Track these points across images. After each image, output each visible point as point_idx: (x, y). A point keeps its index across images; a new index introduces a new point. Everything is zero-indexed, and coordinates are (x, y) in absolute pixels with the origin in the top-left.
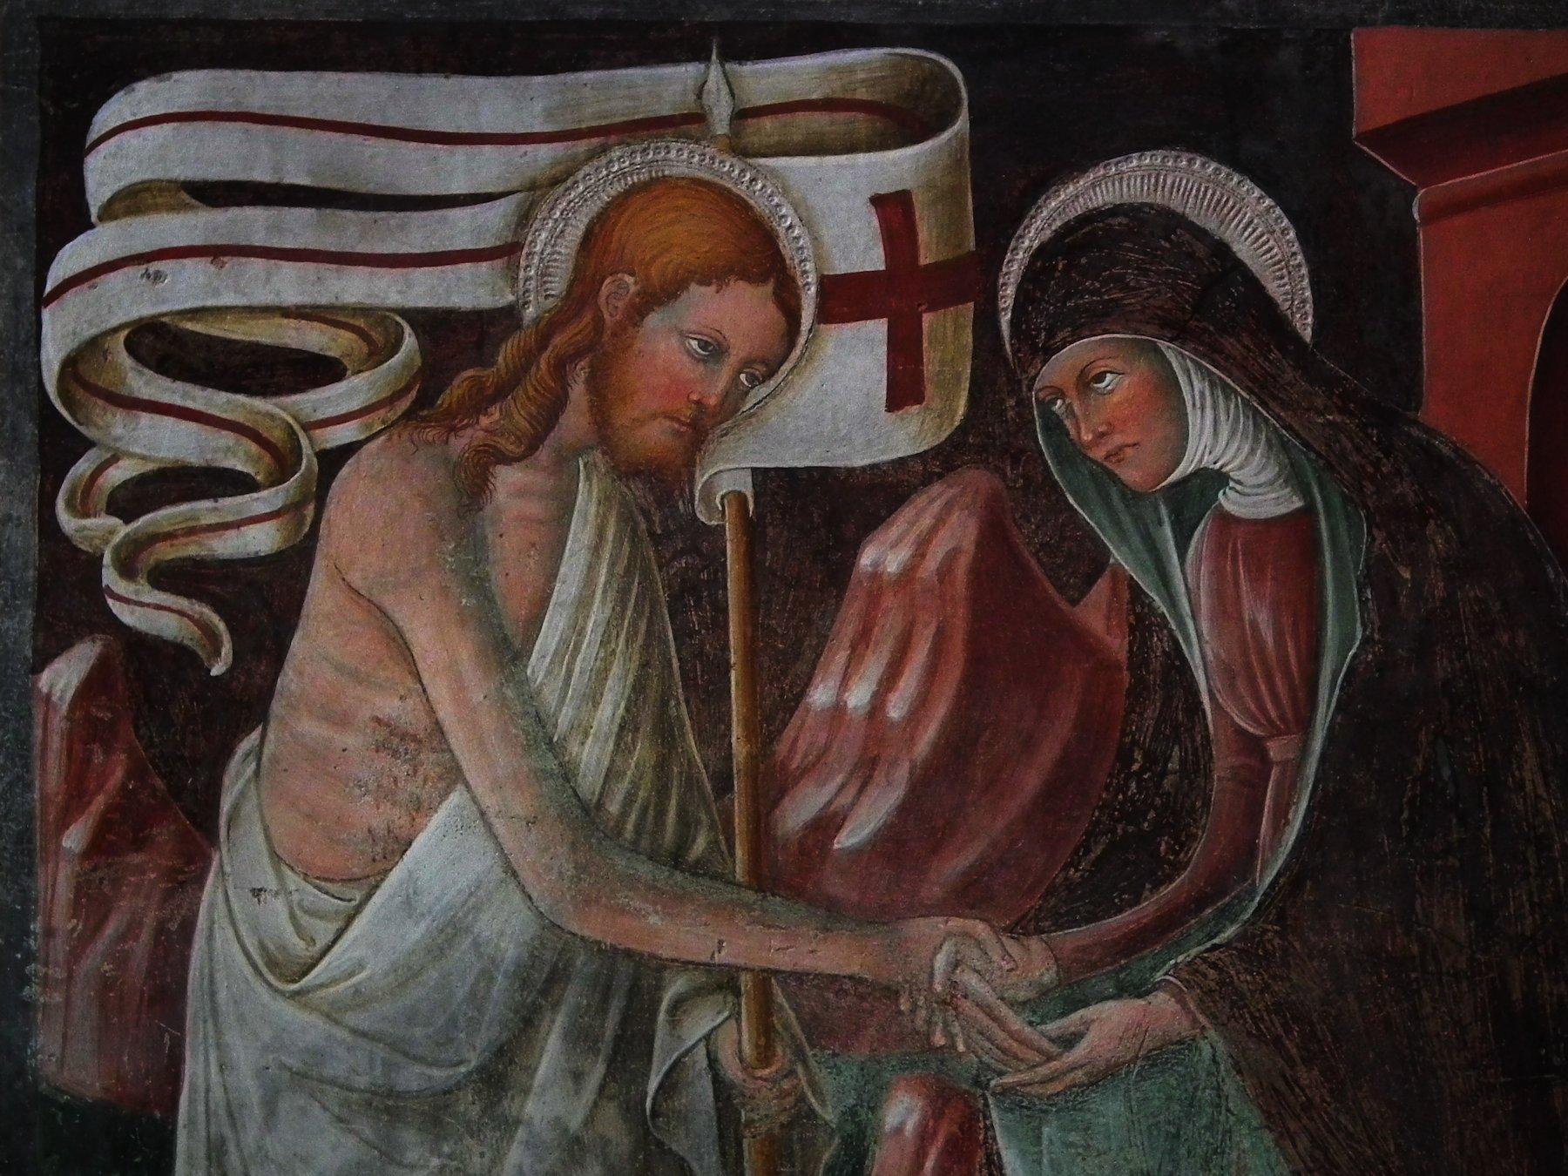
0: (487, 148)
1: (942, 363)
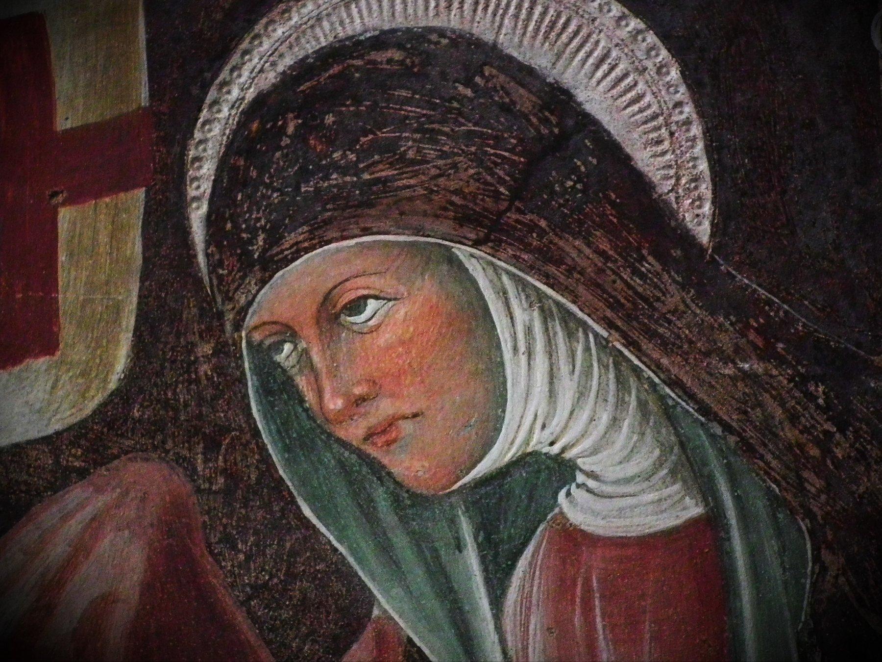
1: (91, 286)
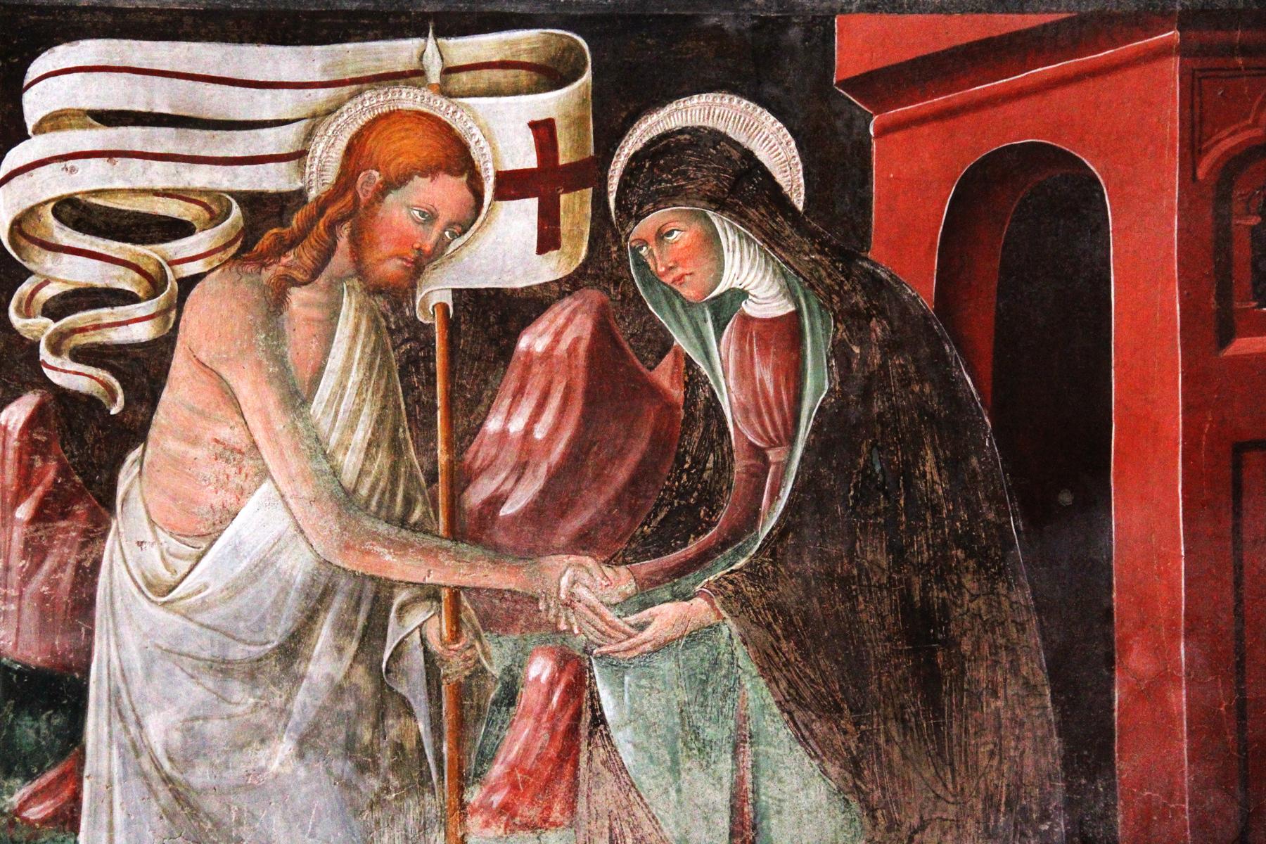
0: (285, 91)
1: (572, 224)
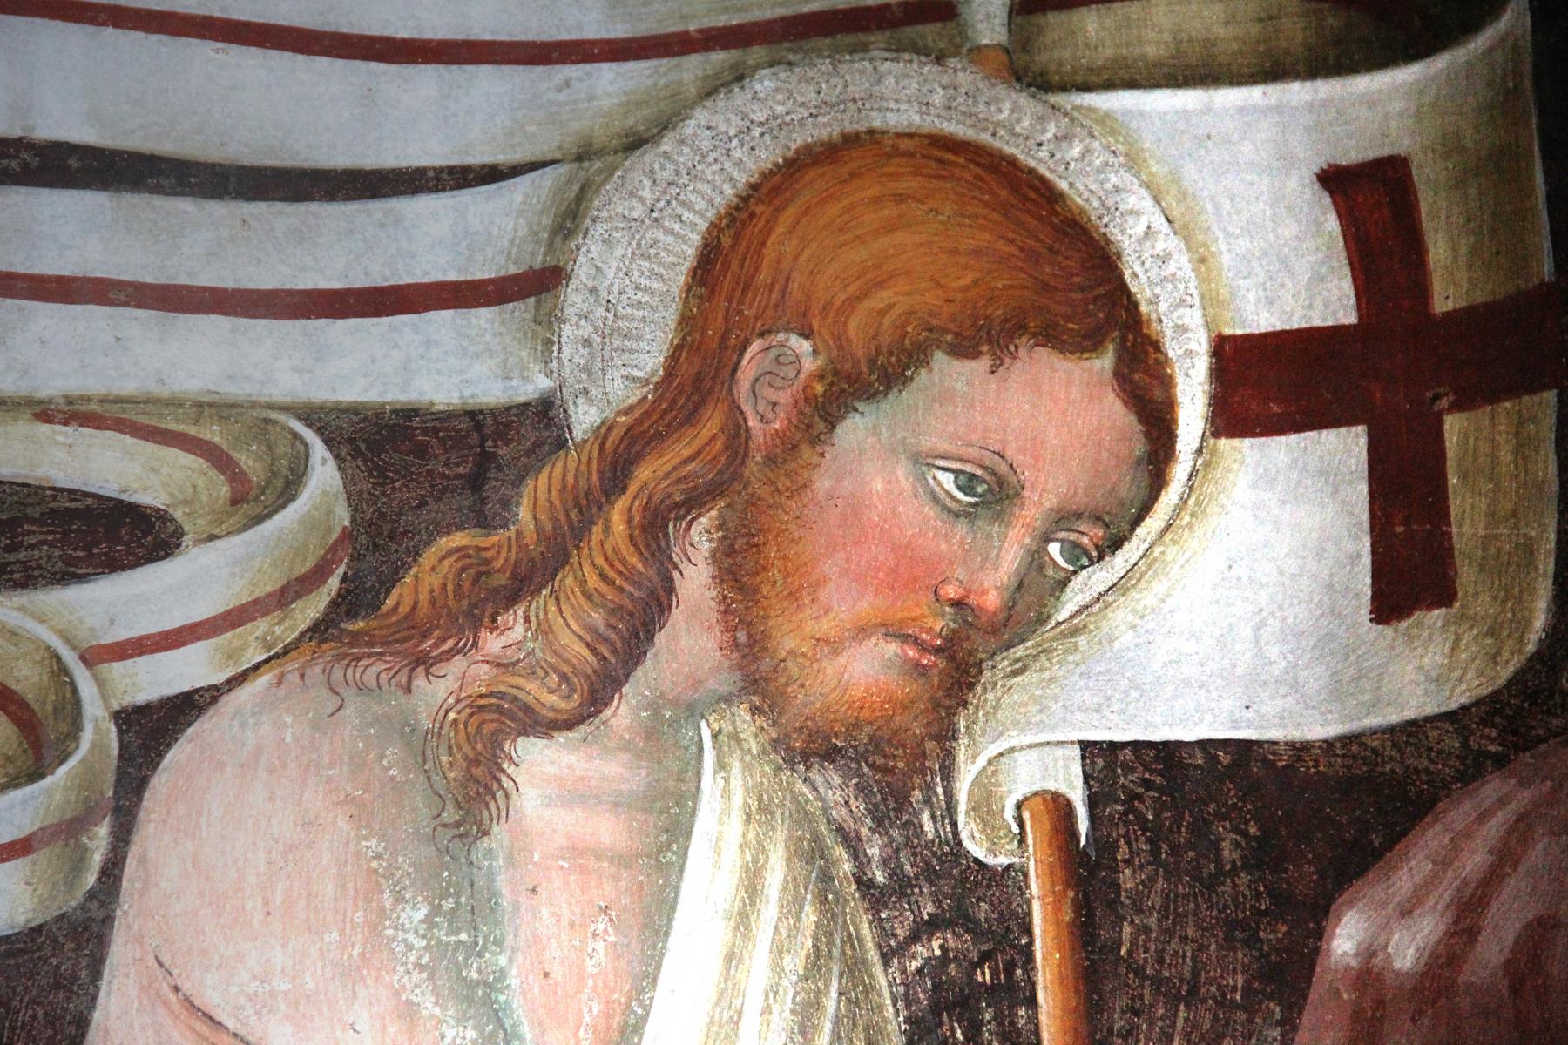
0: (485, 71)
